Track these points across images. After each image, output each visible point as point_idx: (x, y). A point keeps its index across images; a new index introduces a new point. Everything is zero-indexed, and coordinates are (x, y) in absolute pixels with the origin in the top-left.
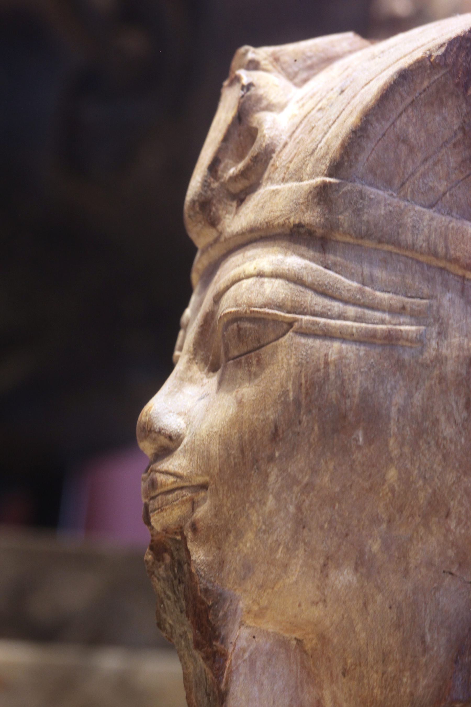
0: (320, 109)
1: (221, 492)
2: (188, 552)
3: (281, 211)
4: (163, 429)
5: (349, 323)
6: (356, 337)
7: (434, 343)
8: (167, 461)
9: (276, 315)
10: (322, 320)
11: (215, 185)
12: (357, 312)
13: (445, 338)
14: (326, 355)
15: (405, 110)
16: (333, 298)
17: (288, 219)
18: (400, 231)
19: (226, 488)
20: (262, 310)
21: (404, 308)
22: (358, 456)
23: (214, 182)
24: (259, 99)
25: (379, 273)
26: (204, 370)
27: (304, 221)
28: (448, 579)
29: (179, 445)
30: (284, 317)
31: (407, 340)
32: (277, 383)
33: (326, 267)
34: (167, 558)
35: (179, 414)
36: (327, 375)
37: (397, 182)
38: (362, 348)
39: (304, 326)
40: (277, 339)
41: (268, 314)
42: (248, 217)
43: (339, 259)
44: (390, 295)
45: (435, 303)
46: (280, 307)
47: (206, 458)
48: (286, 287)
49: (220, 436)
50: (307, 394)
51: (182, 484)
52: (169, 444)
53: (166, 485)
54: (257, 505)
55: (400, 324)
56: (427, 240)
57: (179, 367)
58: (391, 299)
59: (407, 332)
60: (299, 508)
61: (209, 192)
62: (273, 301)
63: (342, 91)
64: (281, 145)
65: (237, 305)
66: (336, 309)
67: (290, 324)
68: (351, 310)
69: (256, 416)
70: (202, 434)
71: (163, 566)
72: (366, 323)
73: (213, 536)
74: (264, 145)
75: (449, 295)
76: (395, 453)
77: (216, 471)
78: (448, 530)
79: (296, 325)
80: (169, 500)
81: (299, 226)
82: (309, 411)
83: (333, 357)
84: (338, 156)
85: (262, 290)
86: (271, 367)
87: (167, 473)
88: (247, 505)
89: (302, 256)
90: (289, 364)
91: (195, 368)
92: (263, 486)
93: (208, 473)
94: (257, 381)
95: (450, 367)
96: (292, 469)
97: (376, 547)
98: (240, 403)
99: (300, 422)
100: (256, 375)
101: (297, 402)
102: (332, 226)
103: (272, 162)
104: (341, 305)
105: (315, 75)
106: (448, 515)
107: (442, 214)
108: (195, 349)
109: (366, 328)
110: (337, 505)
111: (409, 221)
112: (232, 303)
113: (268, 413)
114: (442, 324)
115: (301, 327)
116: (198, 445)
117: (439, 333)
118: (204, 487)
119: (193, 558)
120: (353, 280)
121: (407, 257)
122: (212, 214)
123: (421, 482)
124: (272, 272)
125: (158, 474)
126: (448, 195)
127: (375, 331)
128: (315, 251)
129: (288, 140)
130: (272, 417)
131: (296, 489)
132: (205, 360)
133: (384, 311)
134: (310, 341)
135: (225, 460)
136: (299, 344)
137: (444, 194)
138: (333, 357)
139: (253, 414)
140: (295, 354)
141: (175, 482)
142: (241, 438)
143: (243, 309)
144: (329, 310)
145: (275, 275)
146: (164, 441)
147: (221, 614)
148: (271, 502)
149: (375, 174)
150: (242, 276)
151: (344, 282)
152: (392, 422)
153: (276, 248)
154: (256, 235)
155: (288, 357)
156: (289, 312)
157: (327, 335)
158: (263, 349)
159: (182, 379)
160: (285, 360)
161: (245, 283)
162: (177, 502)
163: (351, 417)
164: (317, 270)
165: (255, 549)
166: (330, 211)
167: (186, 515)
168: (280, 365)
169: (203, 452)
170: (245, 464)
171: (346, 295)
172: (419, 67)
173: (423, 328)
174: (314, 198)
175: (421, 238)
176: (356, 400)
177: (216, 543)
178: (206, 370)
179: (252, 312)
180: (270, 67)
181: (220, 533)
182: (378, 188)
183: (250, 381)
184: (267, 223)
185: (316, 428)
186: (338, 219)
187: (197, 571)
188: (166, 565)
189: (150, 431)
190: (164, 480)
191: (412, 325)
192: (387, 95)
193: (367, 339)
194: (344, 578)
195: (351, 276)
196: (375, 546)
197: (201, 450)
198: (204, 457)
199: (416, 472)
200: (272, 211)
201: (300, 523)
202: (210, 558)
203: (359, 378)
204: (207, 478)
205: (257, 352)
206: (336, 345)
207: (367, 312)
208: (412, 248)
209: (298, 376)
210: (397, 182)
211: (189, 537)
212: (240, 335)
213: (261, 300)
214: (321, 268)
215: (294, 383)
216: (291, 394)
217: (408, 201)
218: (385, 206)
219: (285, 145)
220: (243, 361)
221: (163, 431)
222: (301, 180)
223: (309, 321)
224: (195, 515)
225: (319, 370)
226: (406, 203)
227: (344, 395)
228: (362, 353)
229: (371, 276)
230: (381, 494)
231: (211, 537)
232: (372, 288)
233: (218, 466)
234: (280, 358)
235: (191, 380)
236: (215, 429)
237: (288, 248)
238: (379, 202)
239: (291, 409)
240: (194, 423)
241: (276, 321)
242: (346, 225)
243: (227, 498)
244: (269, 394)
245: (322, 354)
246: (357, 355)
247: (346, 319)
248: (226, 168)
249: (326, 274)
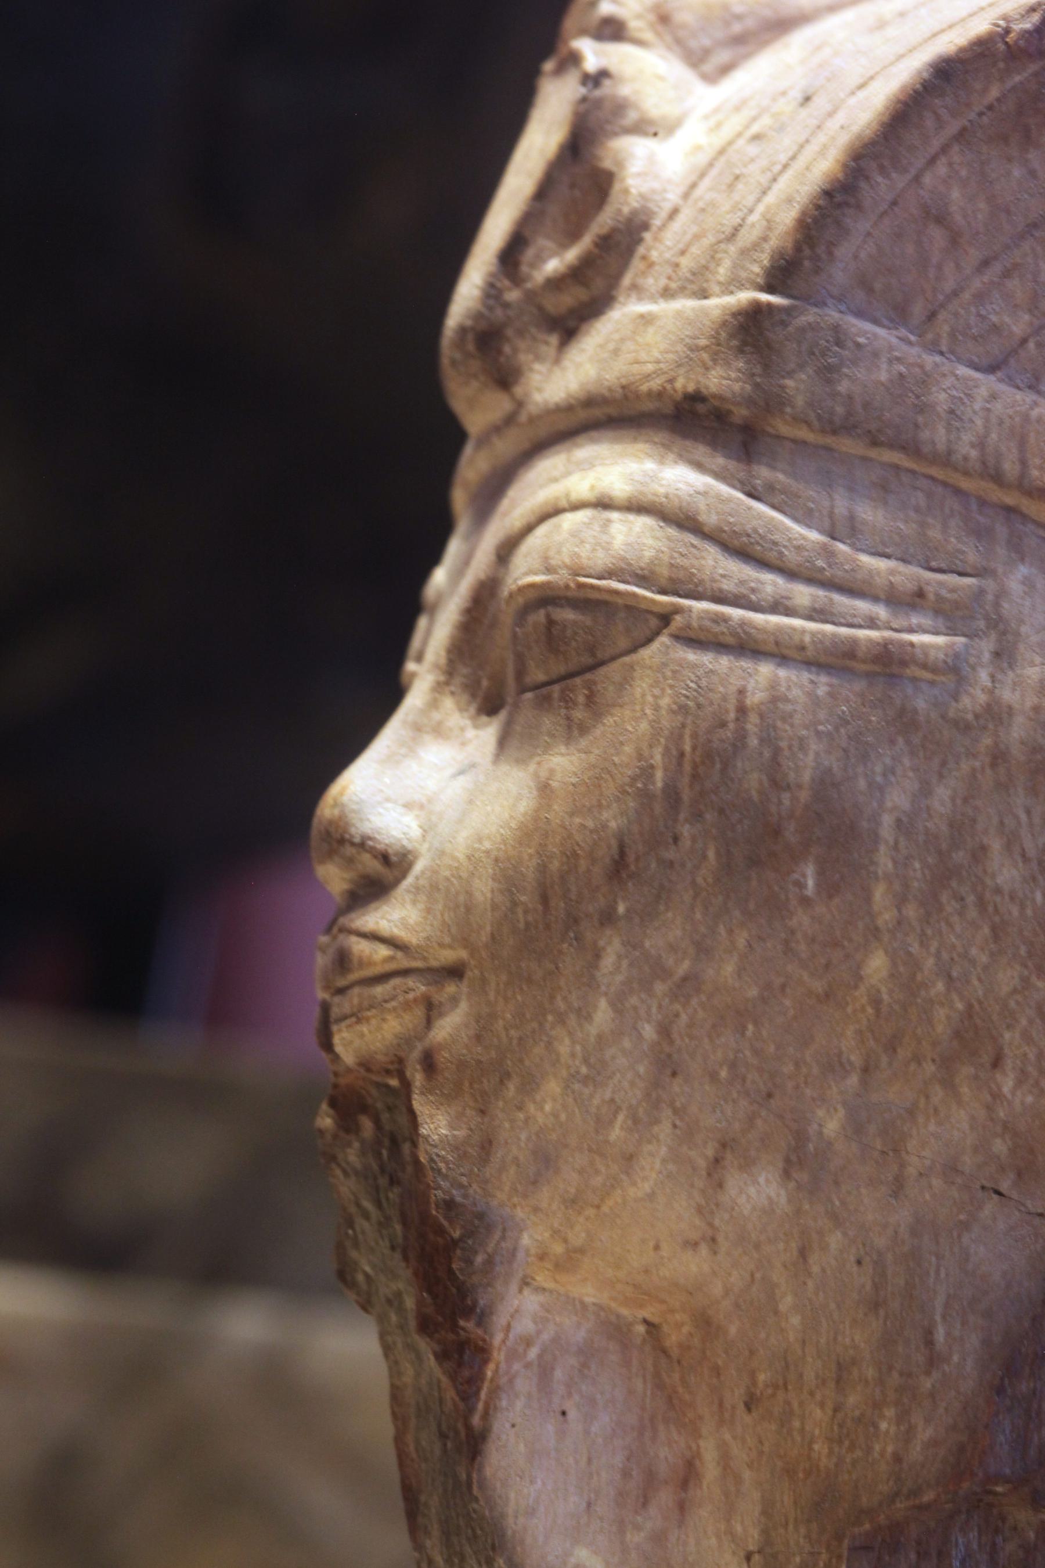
0: (757, 138)
1: (493, 985)
3: (658, 362)
4: (370, 838)
5: (797, 622)
6: (810, 653)
7: (984, 676)
8: (376, 909)
9: (634, 595)
10: (736, 613)
11: (513, 295)
12: (815, 598)
13: (1011, 666)
14: (742, 692)
15: (944, 149)
16: (764, 564)
17: (671, 381)
18: (920, 419)
19: (504, 977)
21: (920, 594)
22: (801, 920)
23: (510, 289)
24: (620, 107)
25: (869, 513)
26: (466, 710)
27: (707, 388)
28: (990, 1207)
29: (404, 875)
30: (653, 601)
31: (924, 666)
33: (750, 495)
34: (367, 1125)
35: (408, 806)
36: (741, 736)
37: (918, 310)
38: (823, 679)
39: (695, 624)
40: (634, 649)
41: (617, 592)
43: (781, 477)
44: (892, 564)
45: (990, 584)
46: (643, 579)
47: (462, 909)
48: (659, 533)
49: (497, 860)
50: (695, 777)
51: (409, 964)
52: (381, 872)
53: (370, 963)
54: (572, 1020)
55: (911, 630)
56: (981, 444)
57: (415, 700)
58: (892, 572)
59: (925, 647)
60: (665, 1031)
61: (499, 312)
62: (630, 564)
63: (807, 99)
64: (663, 215)
65: (549, 570)
66: (769, 589)
67: (665, 618)
68: (803, 594)
69: (578, 820)
71: (356, 1145)
72: (834, 623)
73: (471, 1084)
74: (626, 210)
75: (1023, 570)
76: (886, 917)
77: (484, 939)
78: (997, 1095)
79: (678, 620)
80: (375, 997)
81: (696, 398)
82: (697, 816)
83: (756, 697)
84: (789, 245)
85: (605, 538)
86: (616, 711)
87: (374, 937)
88: (550, 1018)
89: (699, 466)
90: (657, 708)
91: (448, 703)
92: (588, 980)
93: (465, 942)
94: (583, 743)
95: (1018, 731)
96: (653, 942)
97: (832, 1126)
98: (544, 789)
99: (676, 839)
100: (584, 730)
101: (672, 794)
102: (770, 403)
103: (641, 250)
104: (780, 581)
105: (747, 56)
106: (997, 1063)
107: (1018, 388)
108: (451, 662)
109: (834, 635)
110: (750, 1027)
111: (940, 398)
112: (537, 564)
113: (605, 815)
114: (1004, 633)
115: (689, 627)
116: (448, 879)
117: (997, 655)
118: (455, 972)
119: (423, 1131)
120: (809, 526)
121: (933, 479)
122: (502, 359)
123: (940, 986)
124: (629, 500)
125: (354, 939)
126: (1031, 345)
127: (854, 642)
128: (728, 457)
129: (681, 202)
130: (613, 824)
131: (660, 988)
132: (472, 688)
133: (875, 599)
134: (706, 659)
135: (506, 915)
136: (682, 664)
137: (1024, 341)
138: (756, 697)
139: (572, 814)
140: (671, 687)
141: (391, 959)
142: (542, 869)
143: (561, 578)
144: (753, 591)
145: (636, 507)
146: (371, 865)
147: (479, 1259)
148: (603, 1014)
149: (870, 291)
150: (564, 503)
151: (788, 529)
152: (882, 848)
153: (641, 446)
154: (597, 413)
155: (657, 691)
156: (663, 592)
157: (746, 646)
158: (603, 671)
159: (418, 728)
160: (650, 699)
161: (569, 521)
162: (394, 1004)
163: (791, 833)
164: (729, 500)
165: (563, 1117)
166: (766, 367)
167: (412, 1033)
168: (638, 708)
169: (457, 893)
170: (548, 927)
171: (792, 558)
172: (982, 55)
173: (961, 640)
174: (732, 336)
175: (967, 437)
176: (804, 796)
177: (476, 1101)
178: (472, 709)
179: (581, 586)
180: (648, 36)
181: (485, 1079)
182: (876, 322)
183: (569, 740)
184: (623, 387)
185: (711, 854)
186: (783, 387)
187: (432, 1160)
188: (363, 1142)
189: (341, 841)
191: (937, 633)
192: (907, 113)
193: (835, 660)
194: (758, 1190)
195: (805, 518)
196: (832, 1124)
198: (457, 906)
199: (930, 962)
201: (666, 1065)
202: (461, 1133)
203: (814, 746)
204: (463, 954)
205: (588, 676)
206: (766, 670)
207: (838, 598)
208: (945, 460)
209: (677, 737)
210: (918, 310)
211: (418, 1084)
212: (553, 637)
213: (601, 560)
214: (740, 495)
215: (667, 750)
216: (659, 775)
217: (942, 353)
218: (890, 361)
219: (674, 212)
220: (556, 695)
221: (370, 843)
222: (704, 294)
223: (707, 612)
224: (432, 1034)
225: (723, 725)
226: (938, 359)
227: (777, 783)
228: (822, 691)
229: (852, 518)
230: (849, 1010)
231: (467, 1084)
232: (852, 545)
233: (488, 928)
234: (638, 692)
235: (439, 731)
236: (487, 845)
237: (667, 447)
238: (876, 355)
239: (658, 809)
241: (633, 609)
242: (800, 401)
243: (506, 999)
244: (609, 772)
245: (733, 689)
246: (811, 695)
247: (789, 612)
248: (540, 259)
249: (750, 508)
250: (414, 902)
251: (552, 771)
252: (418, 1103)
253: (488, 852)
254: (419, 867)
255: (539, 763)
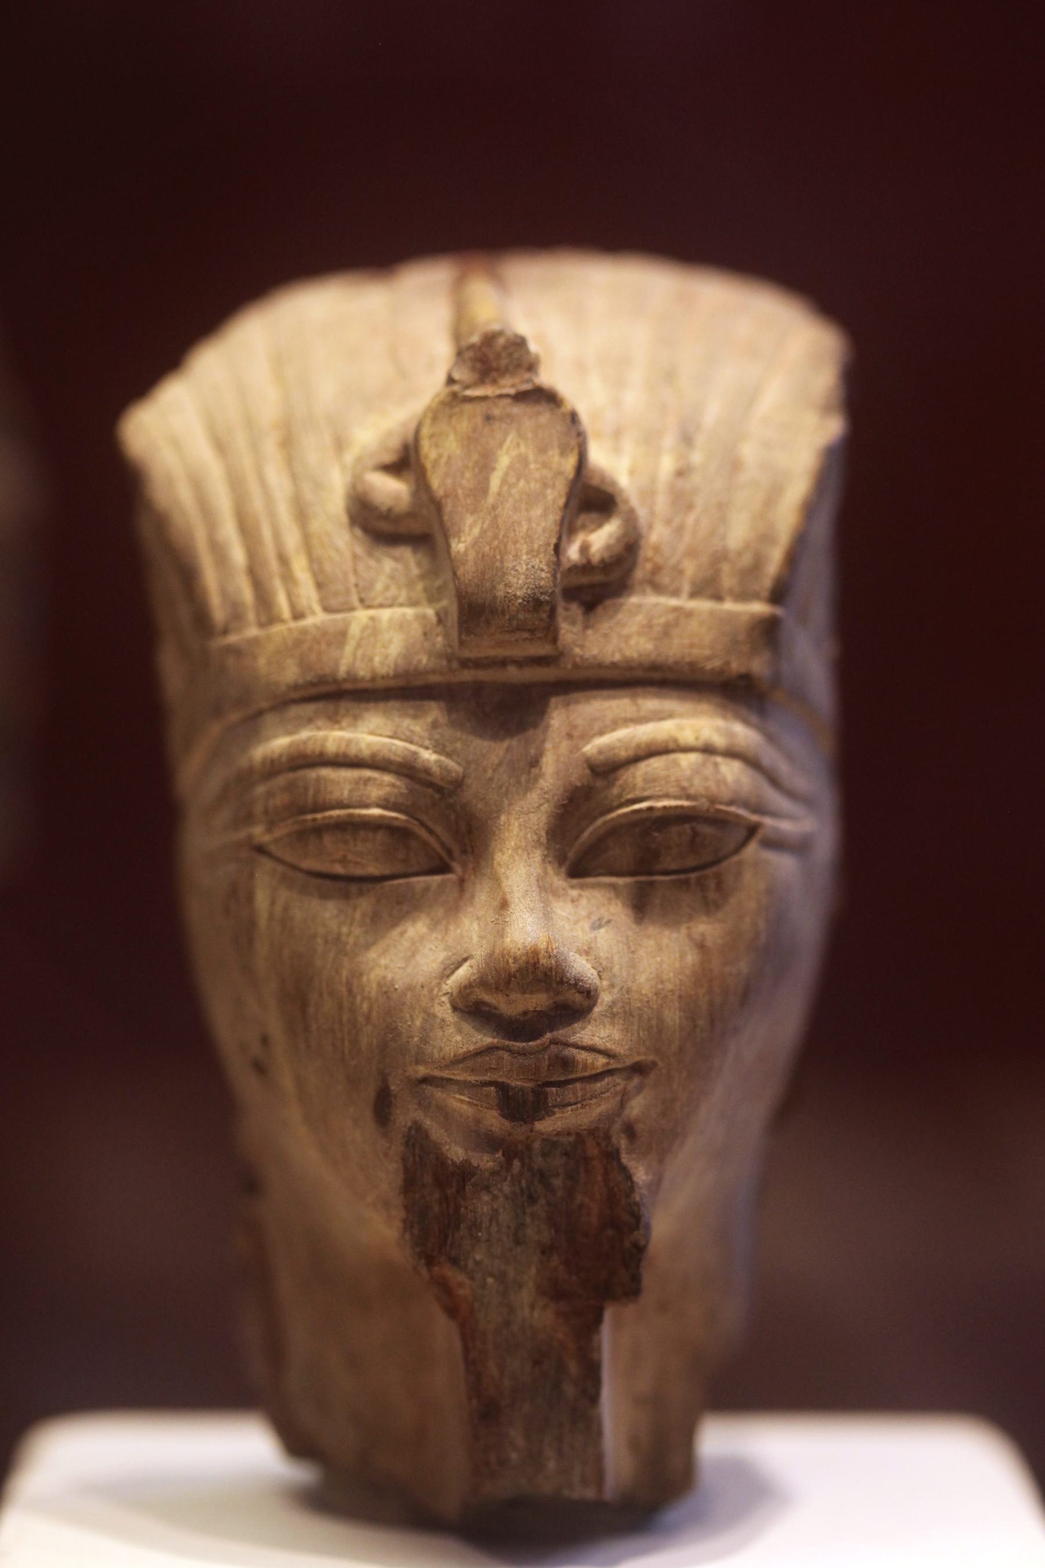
2: (624, 1169)
17: (728, 663)
19: (685, 1074)
20: (733, 809)
32: (747, 919)
42: (633, 642)
46: (746, 805)
47: (655, 1030)
49: (680, 997)
65: (688, 797)
70: (644, 992)
87: (592, 1049)
94: (720, 915)
98: (701, 946)
100: (718, 906)
116: (639, 1009)
118: (638, 1069)
125: (575, 1051)
132: (560, 859)
141: (608, 1064)
143: (703, 804)
145: (731, 753)
150: (671, 746)
153: (704, 707)
154: (657, 675)
158: (725, 864)
169: (649, 1020)
179: (719, 811)
183: (708, 913)
188: (512, 1176)
190: (590, 1061)
197: (645, 1016)
198: (650, 1028)
200: (692, 646)
204: (651, 1057)
205: (715, 869)
212: (695, 843)
213: (725, 794)
219: (651, 527)
224: (627, 1112)
236: (669, 986)
240: (616, 969)
250: (613, 1024)
251: (703, 935)
252: (625, 1159)
253: (672, 991)
254: (605, 998)
255: (689, 928)
